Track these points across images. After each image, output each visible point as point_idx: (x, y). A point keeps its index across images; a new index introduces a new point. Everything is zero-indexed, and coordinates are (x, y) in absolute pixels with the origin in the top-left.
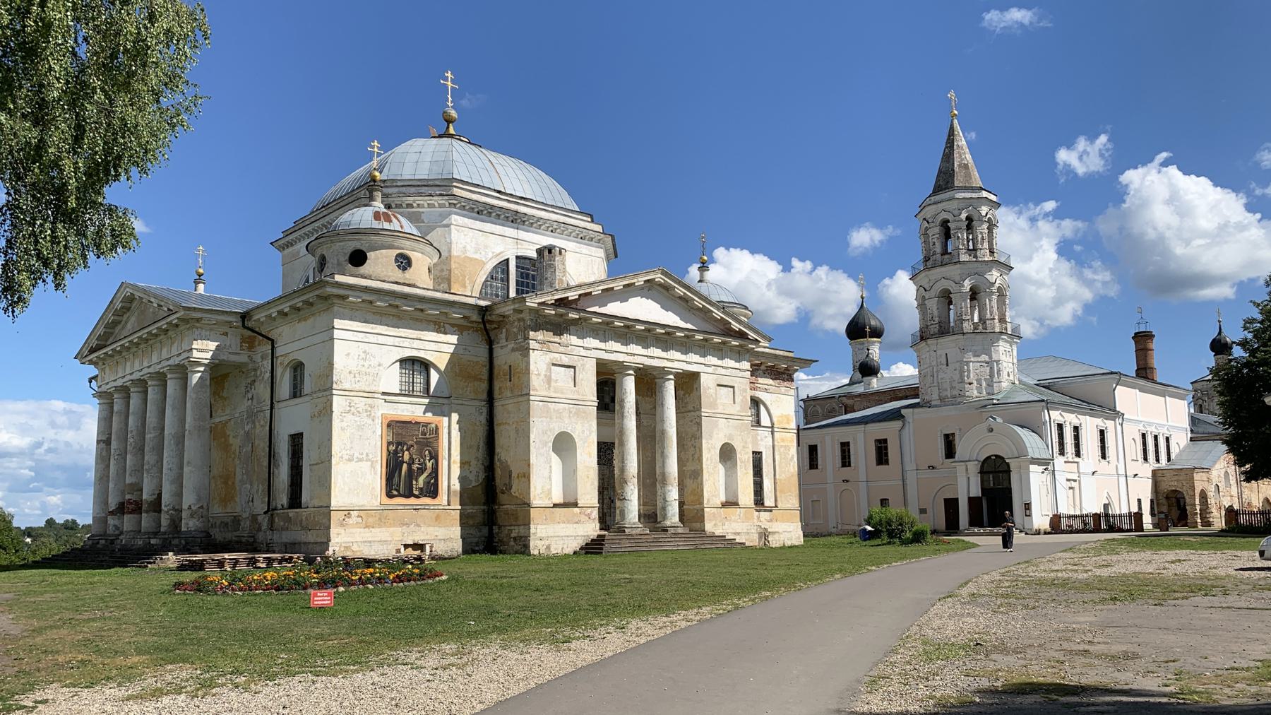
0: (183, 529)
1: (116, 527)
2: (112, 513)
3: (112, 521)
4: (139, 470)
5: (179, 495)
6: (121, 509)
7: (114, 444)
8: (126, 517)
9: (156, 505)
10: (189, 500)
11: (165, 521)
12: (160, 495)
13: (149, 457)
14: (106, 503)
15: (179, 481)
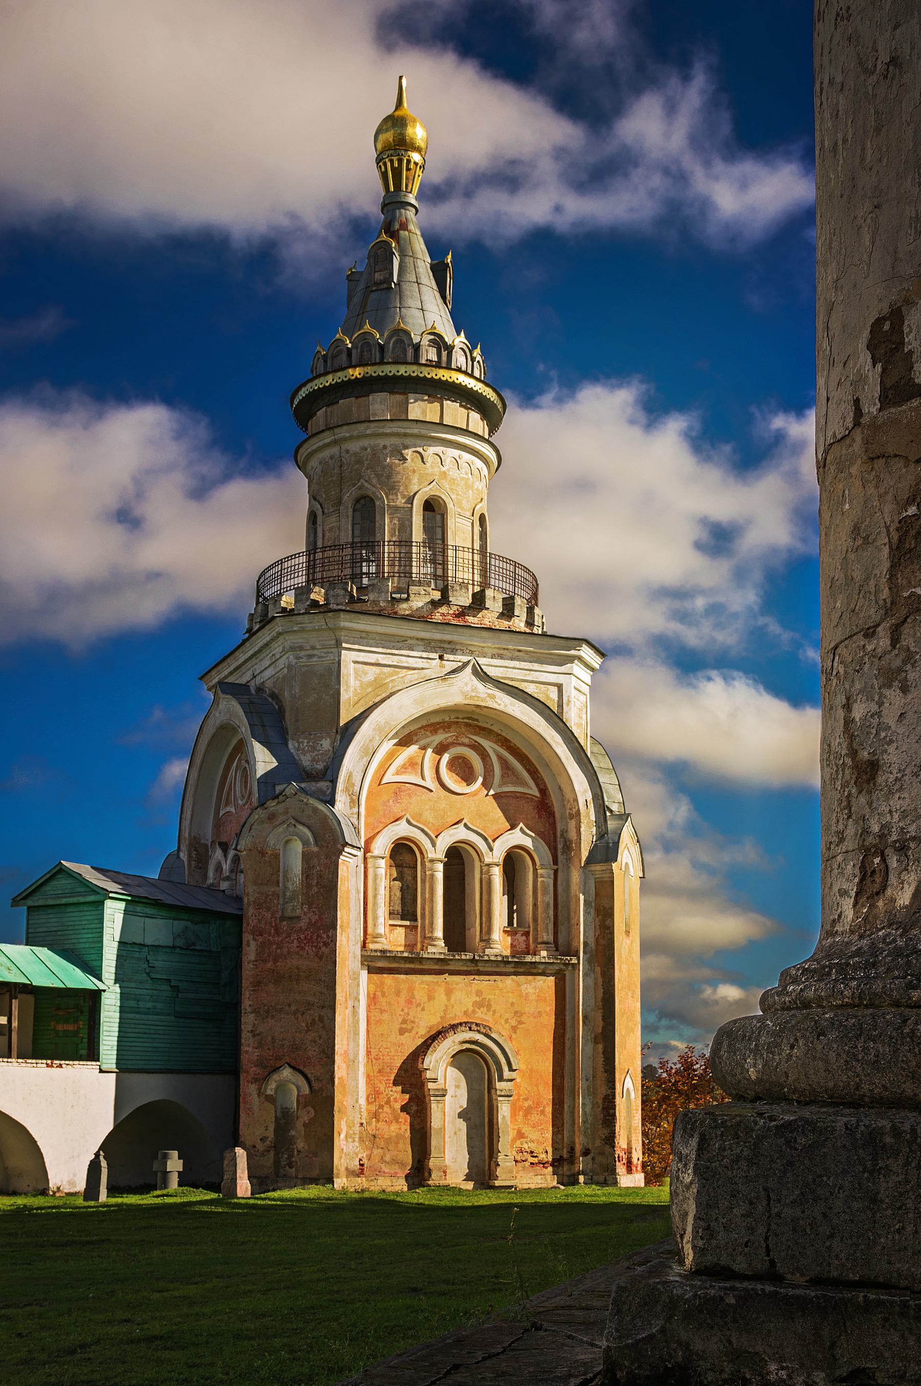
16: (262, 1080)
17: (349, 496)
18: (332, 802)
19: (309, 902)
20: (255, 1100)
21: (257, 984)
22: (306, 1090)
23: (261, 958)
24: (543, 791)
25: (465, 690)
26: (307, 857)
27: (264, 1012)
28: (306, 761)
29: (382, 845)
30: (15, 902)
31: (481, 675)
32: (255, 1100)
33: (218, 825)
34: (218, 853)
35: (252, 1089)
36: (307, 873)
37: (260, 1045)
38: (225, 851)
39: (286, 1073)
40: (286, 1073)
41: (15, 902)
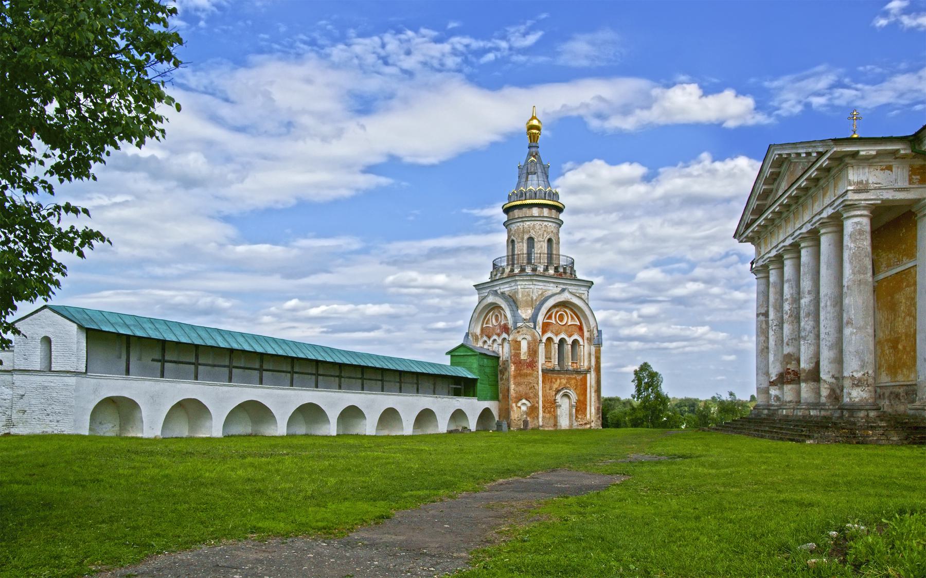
0: (846, 400)
1: (778, 398)
2: (772, 383)
3: (774, 392)
4: (797, 338)
5: (839, 361)
6: (783, 379)
7: (772, 315)
8: (788, 388)
9: (814, 375)
10: (852, 367)
11: (825, 392)
12: (818, 364)
13: (806, 324)
14: (767, 374)
15: (839, 345)
16: (517, 402)
17: (526, 237)
18: (535, 328)
19: (530, 355)
20: (515, 408)
21: (515, 377)
22: (529, 404)
23: (515, 370)
24: (581, 323)
25: (566, 296)
26: (529, 343)
27: (518, 384)
28: (524, 316)
29: (544, 340)
30: (447, 353)
31: (571, 293)
32: (515, 408)
33: (482, 329)
34: (485, 338)
35: (514, 405)
36: (529, 348)
37: (516, 393)
38: (489, 338)
39: (524, 401)
40: (524, 401)
41: (447, 353)
